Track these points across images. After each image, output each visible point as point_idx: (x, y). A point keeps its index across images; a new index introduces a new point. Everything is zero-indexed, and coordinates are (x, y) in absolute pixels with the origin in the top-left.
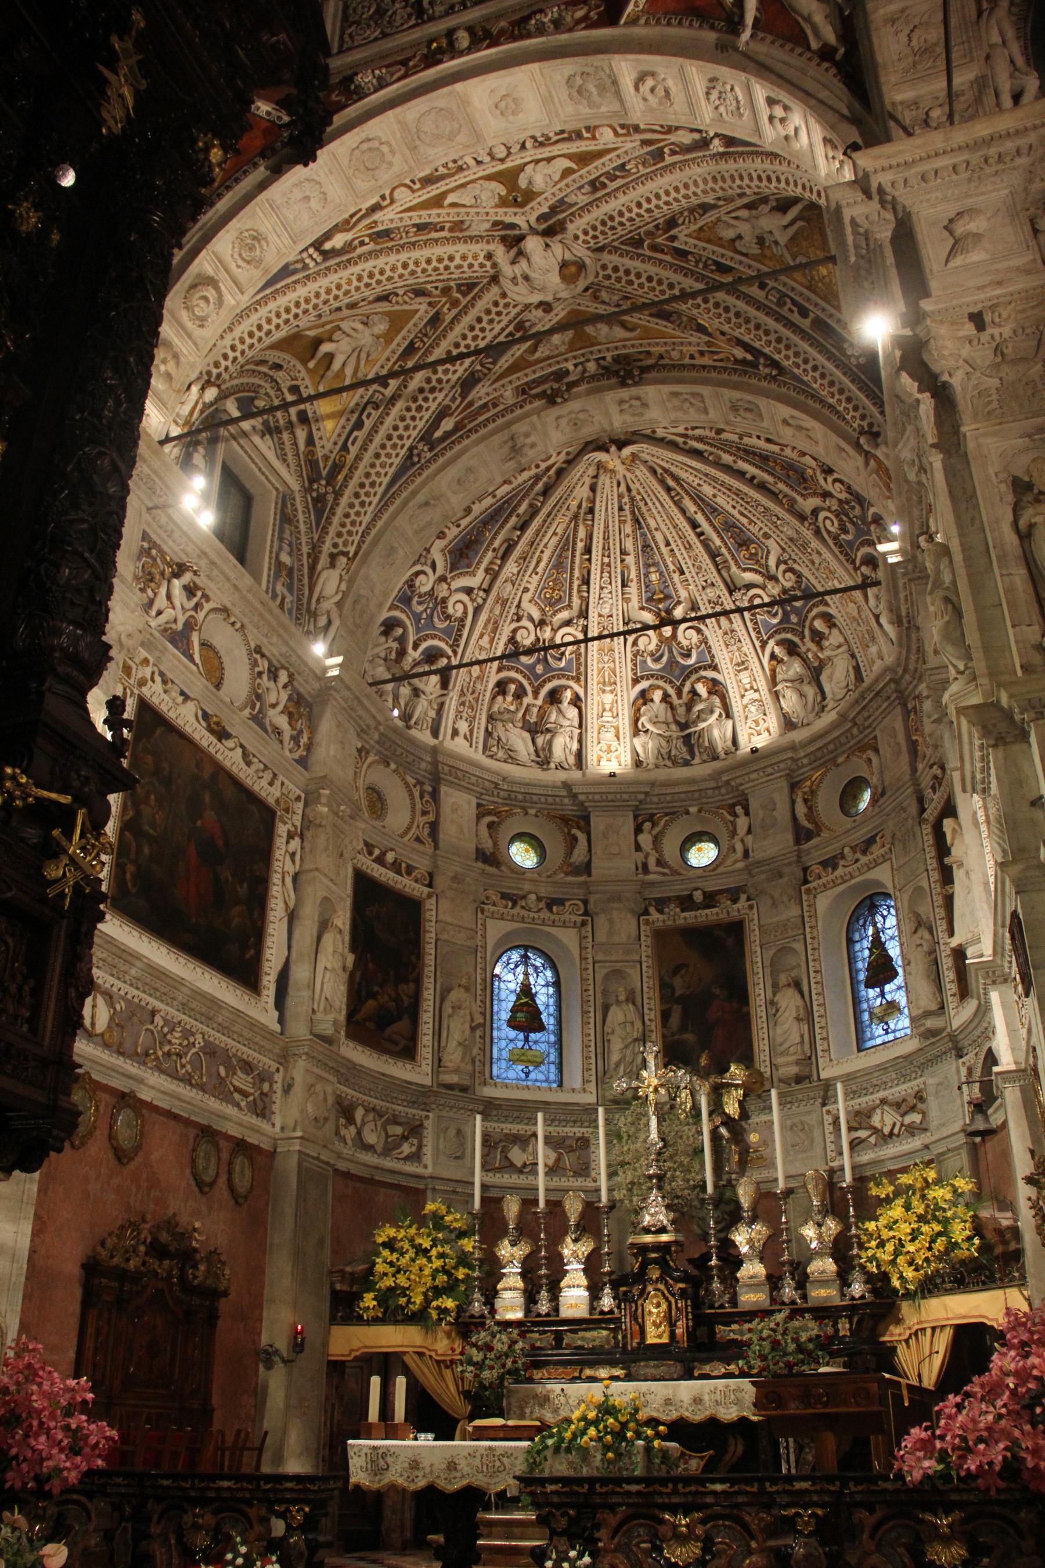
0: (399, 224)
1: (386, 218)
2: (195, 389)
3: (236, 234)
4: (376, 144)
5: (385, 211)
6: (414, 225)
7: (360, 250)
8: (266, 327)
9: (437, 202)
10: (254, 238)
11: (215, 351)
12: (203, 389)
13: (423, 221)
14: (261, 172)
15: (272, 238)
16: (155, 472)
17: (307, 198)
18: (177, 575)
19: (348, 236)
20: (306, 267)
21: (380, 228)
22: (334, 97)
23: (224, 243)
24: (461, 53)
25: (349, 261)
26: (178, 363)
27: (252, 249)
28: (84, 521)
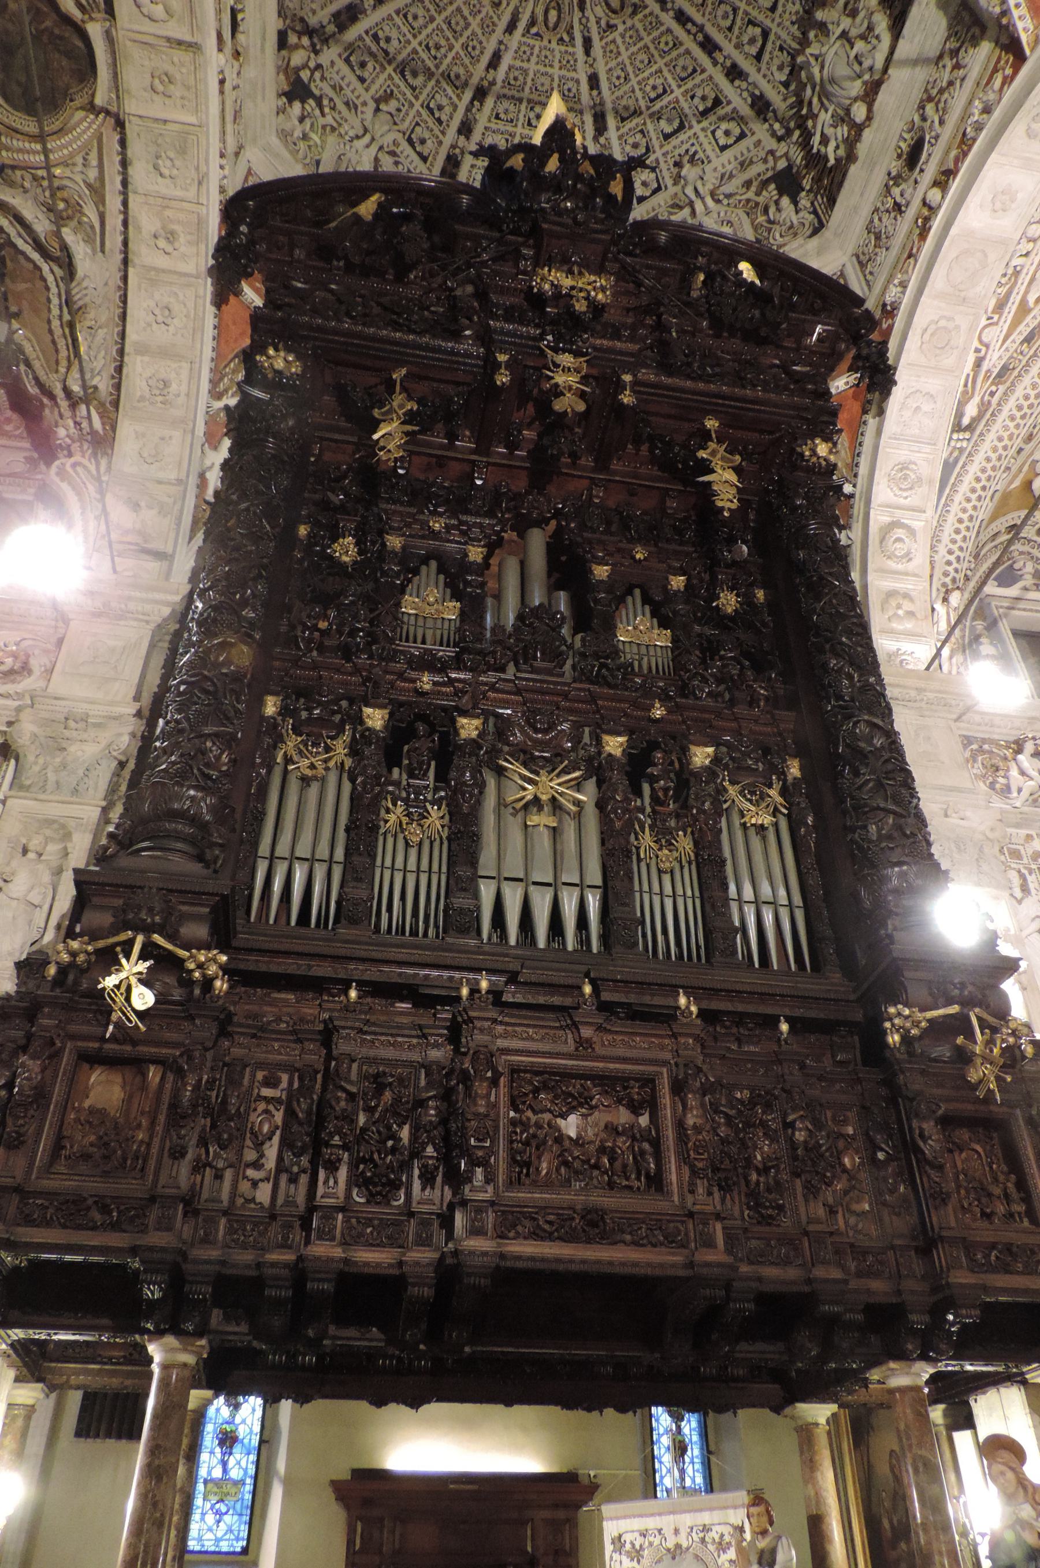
0: (1008, 355)
1: (994, 361)
2: (938, 606)
3: (886, 480)
4: (933, 327)
5: (988, 357)
6: (1022, 343)
7: (995, 400)
8: (965, 516)
9: (1024, 309)
10: (901, 470)
11: (937, 566)
12: (945, 600)
13: (1025, 334)
14: (872, 422)
15: (915, 457)
16: (940, 692)
17: (918, 408)
18: (1019, 751)
19: (976, 399)
20: (961, 450)
21: (996, 371)
22: (885, 326)
23: (883, 492)
24: (940, 206)
25: (993, 414)
26: (911, 600)
27: (905, 478)
28: (868, 781)
